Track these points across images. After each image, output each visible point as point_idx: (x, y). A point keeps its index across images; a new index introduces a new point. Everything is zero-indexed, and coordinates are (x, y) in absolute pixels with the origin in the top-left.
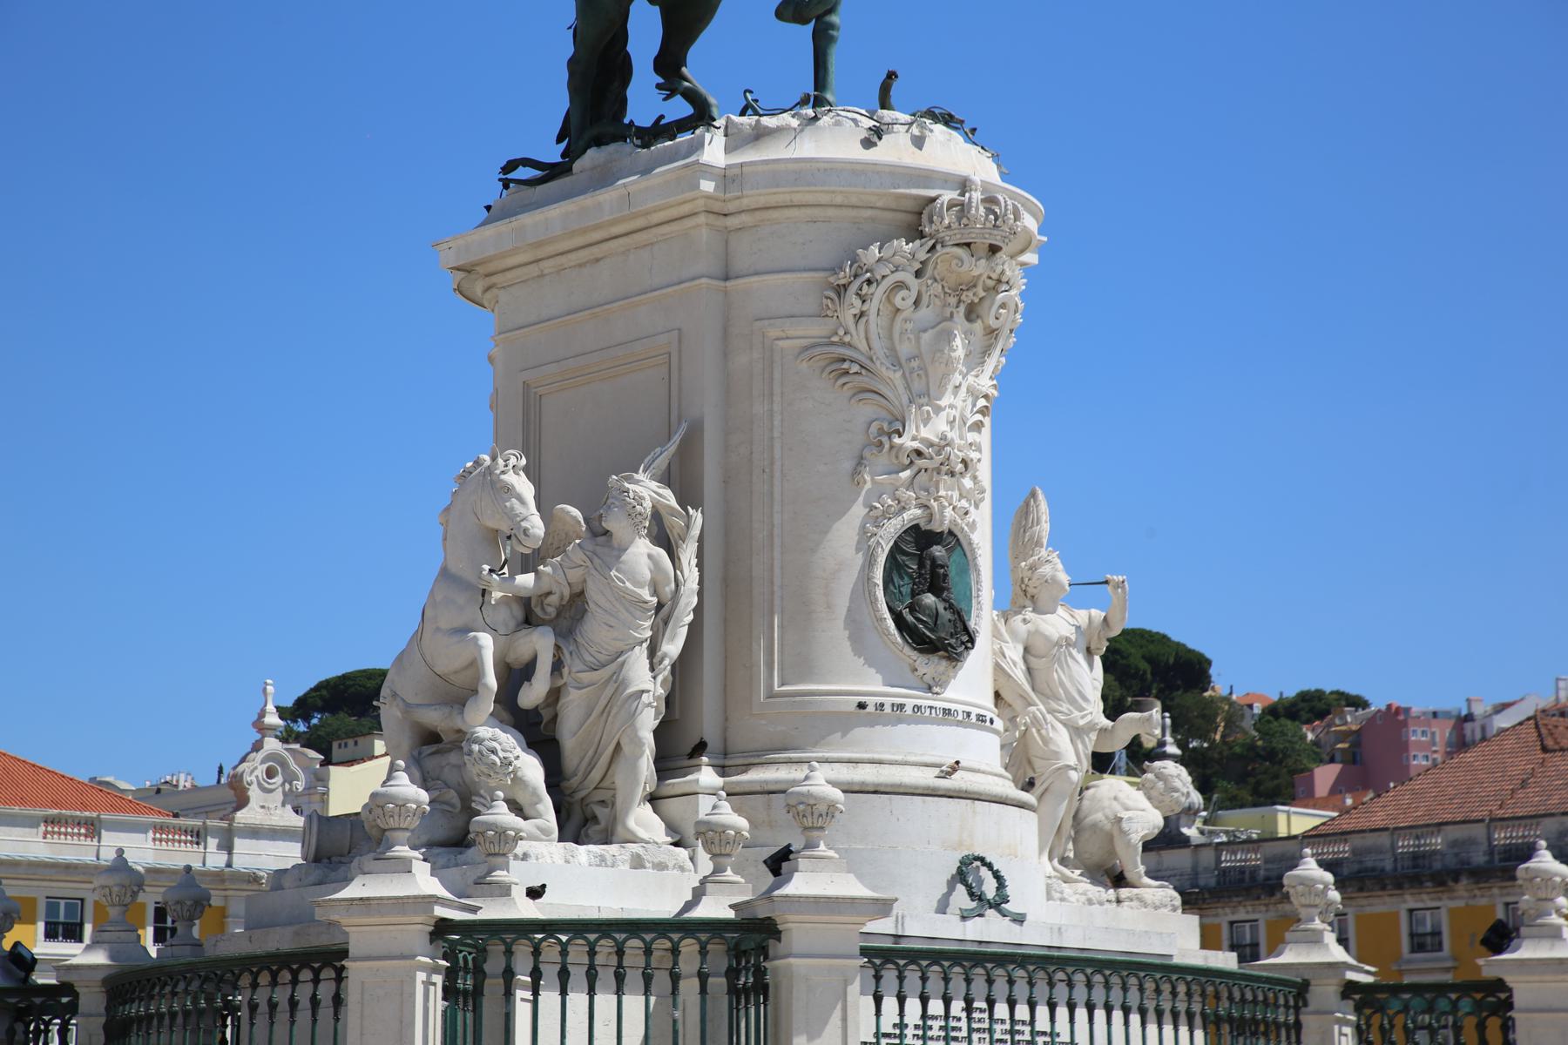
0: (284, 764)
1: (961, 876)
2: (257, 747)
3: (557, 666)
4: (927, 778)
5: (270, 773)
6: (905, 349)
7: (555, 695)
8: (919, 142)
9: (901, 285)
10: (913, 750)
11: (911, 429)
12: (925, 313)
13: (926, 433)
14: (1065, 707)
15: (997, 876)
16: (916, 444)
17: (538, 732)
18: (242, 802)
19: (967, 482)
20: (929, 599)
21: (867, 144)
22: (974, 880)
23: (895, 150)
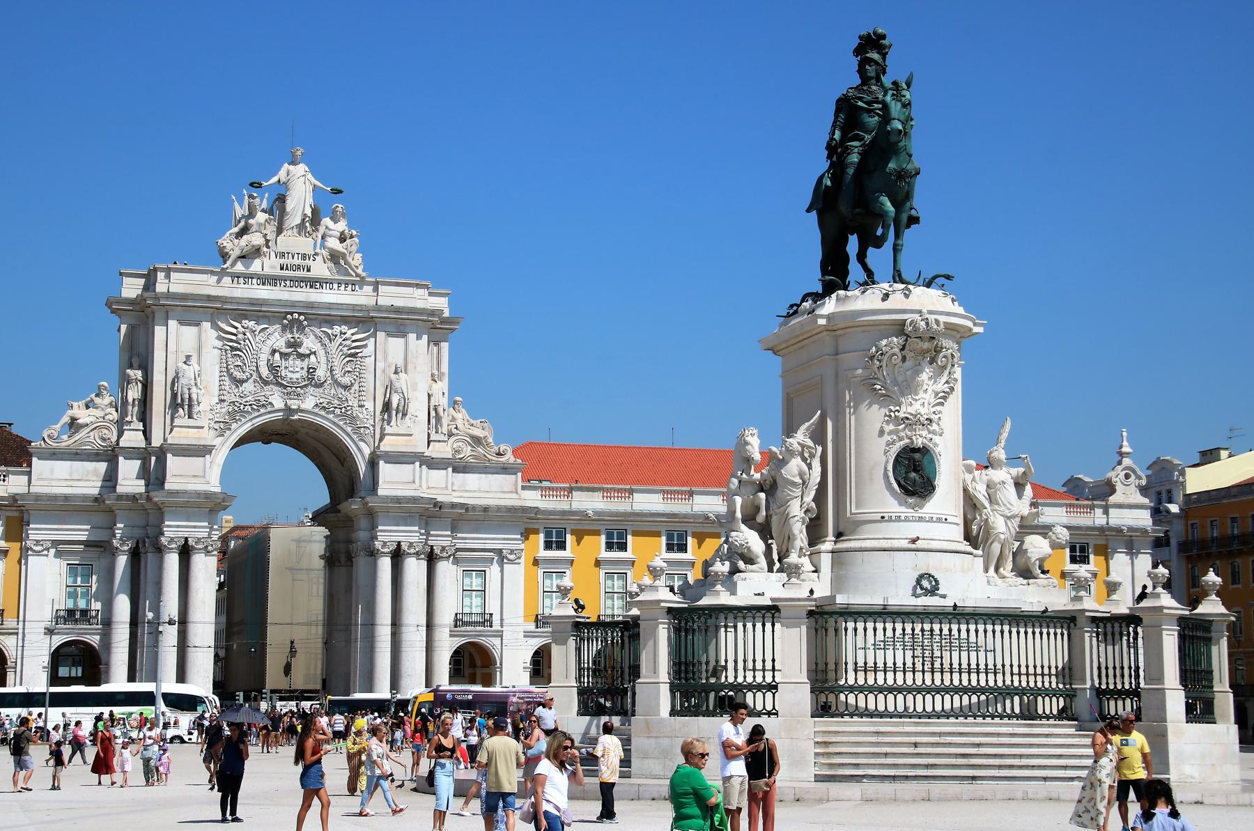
0: (1134, 471)
1: (918, 581)
2: (1120, 463)
3: (767, 509)
4: (905, 544)
5: (1127, 477)
6: (900, 379)
7: (768, 517)
8: (907, 296)
9: (894, 354)
10: (900, 533)
11: (903, 408)
12: (908, 363)
13: (911, 410)
14: (1003, 508)
15: (936, 581)
16: (901, 415)
17: (765, 532)
18: (1112, 490)
19: (935, 427)
20: (913, 475)
21: (883, 300)
22: (927, 584)
23: (897, 301)
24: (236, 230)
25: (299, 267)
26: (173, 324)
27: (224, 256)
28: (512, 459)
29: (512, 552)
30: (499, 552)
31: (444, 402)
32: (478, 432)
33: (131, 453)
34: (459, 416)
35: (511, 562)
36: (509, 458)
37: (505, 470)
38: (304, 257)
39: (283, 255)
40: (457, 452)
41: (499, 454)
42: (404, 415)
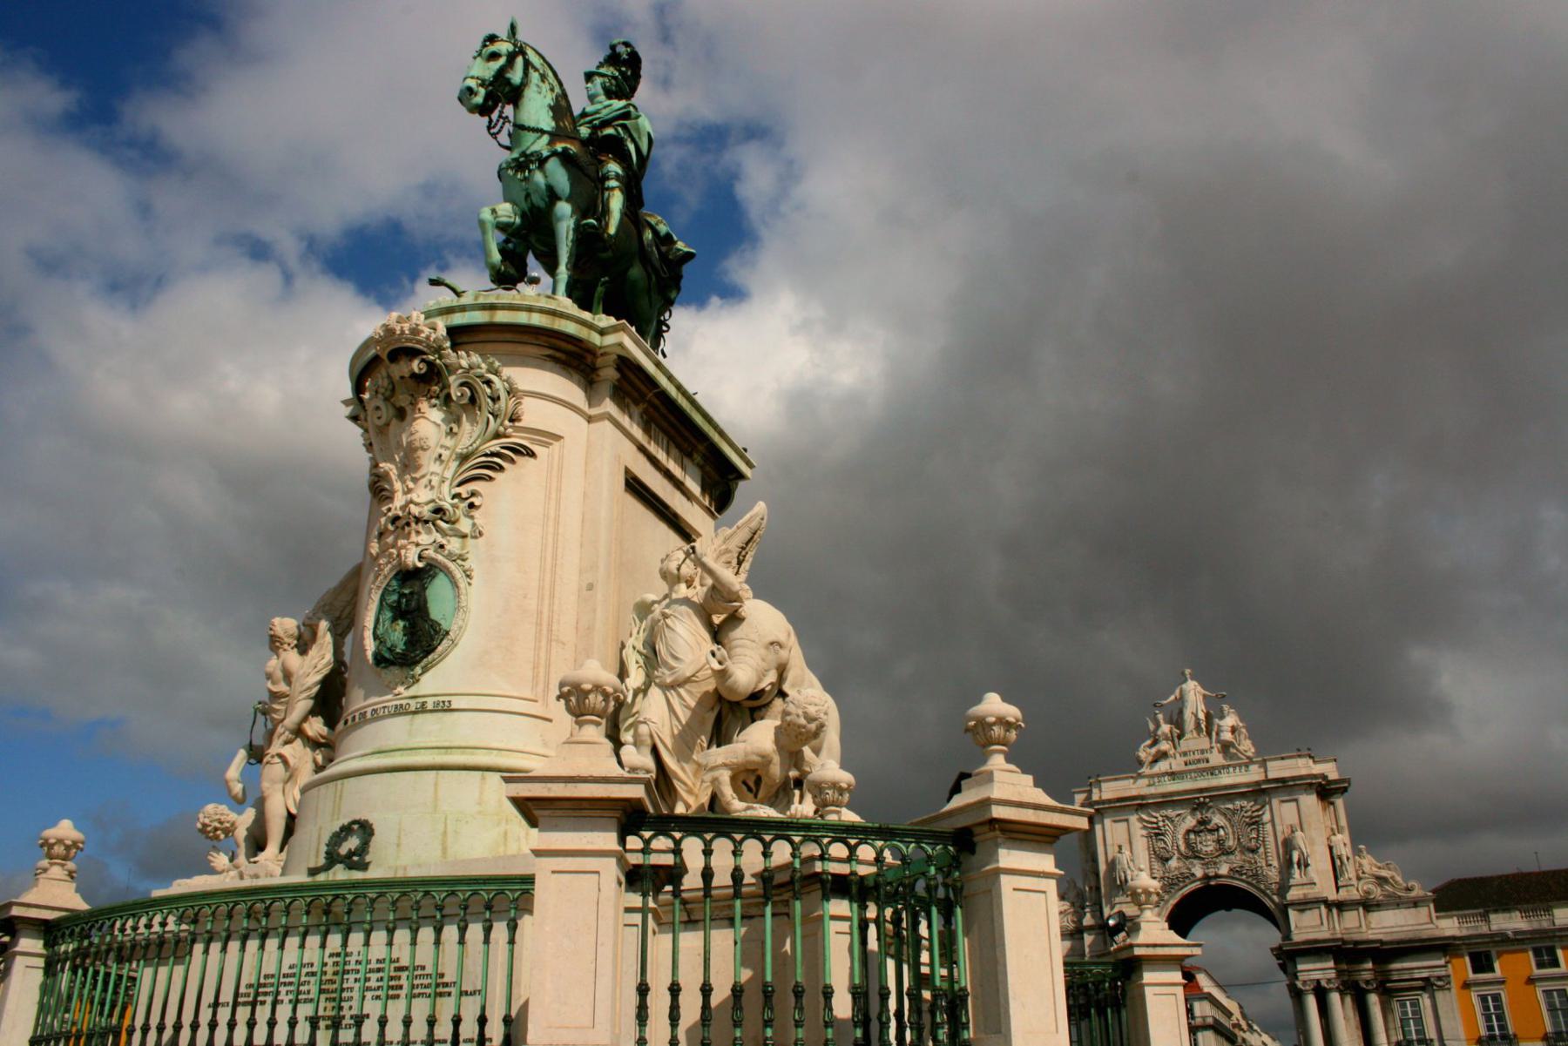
24: (1149, 742)
25: (1199, 761)
26: (1107, 822)
27: (1141, 763)
28: (1421, 893)
29: (1439, 978)
30: (1426, 979)
31: (1344, 850)
32: (1384, 873)
33: (1090, 929)
34: (1365, 862)
35: (1441, 988)
36: (1417, 892)
37: (1415, 903)
38: (1202, 752)
39: (1185, 754)
40: (1368, 893)
41: (1408, 889)
42: (1307, 865)
